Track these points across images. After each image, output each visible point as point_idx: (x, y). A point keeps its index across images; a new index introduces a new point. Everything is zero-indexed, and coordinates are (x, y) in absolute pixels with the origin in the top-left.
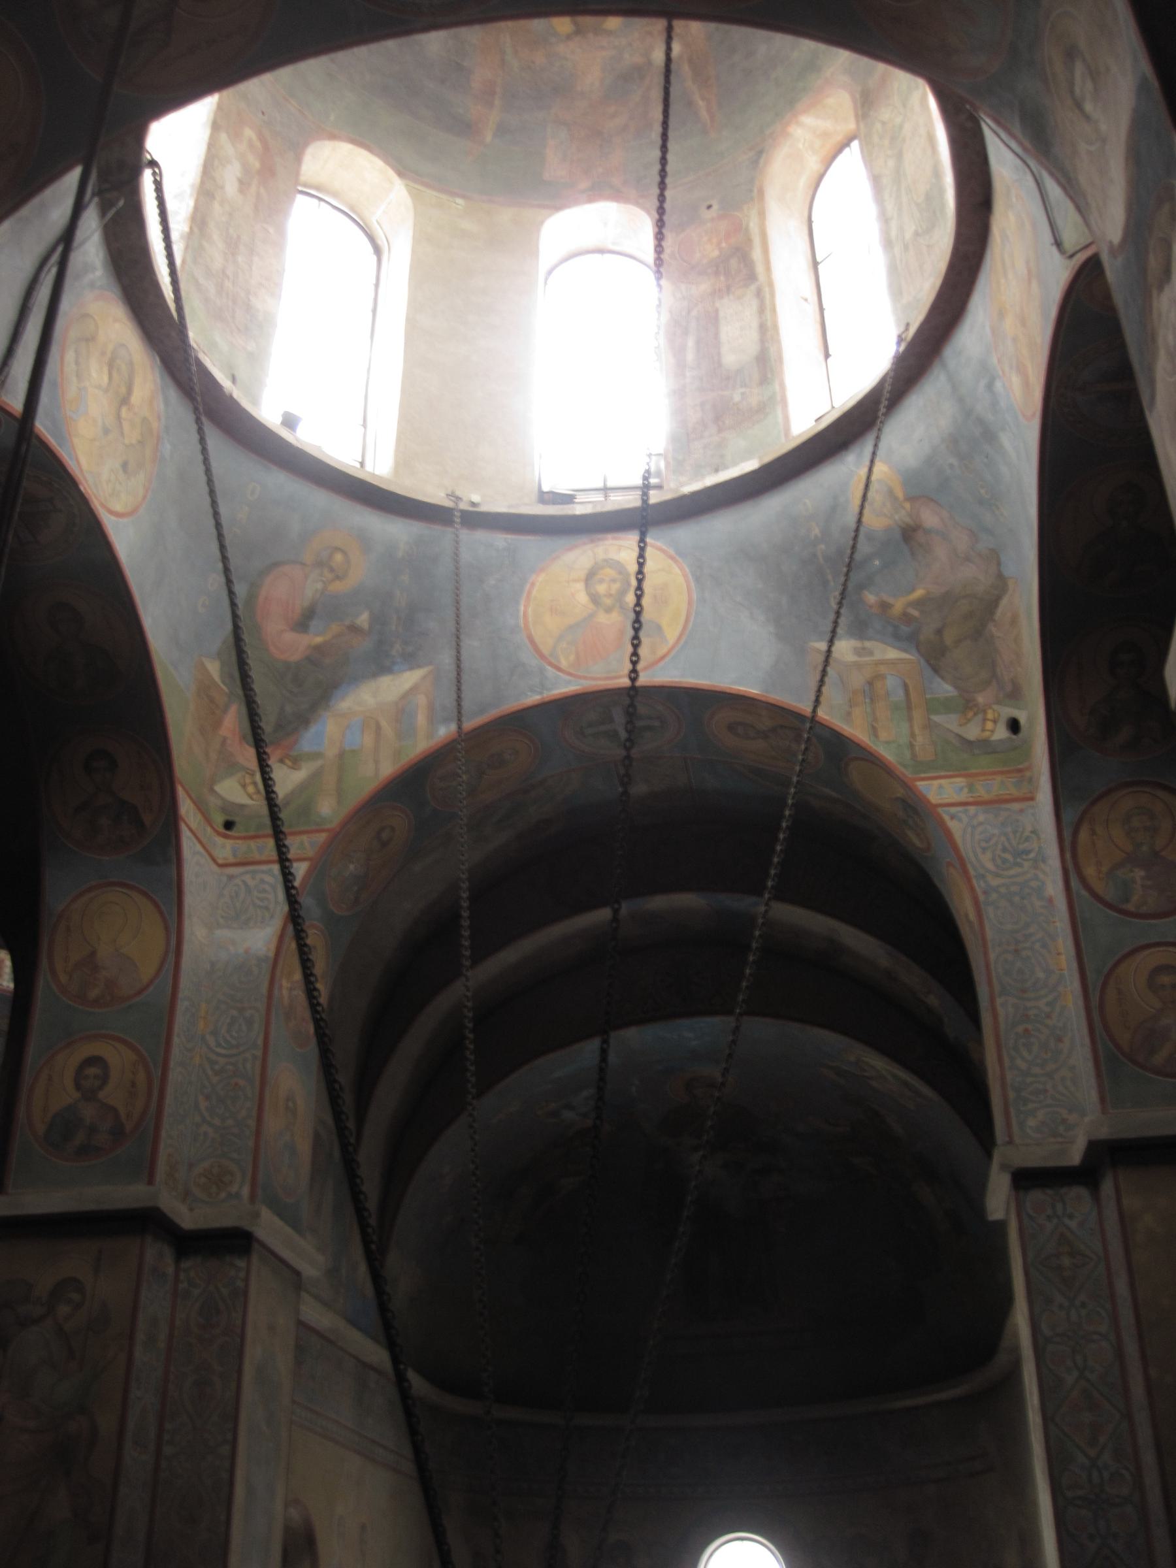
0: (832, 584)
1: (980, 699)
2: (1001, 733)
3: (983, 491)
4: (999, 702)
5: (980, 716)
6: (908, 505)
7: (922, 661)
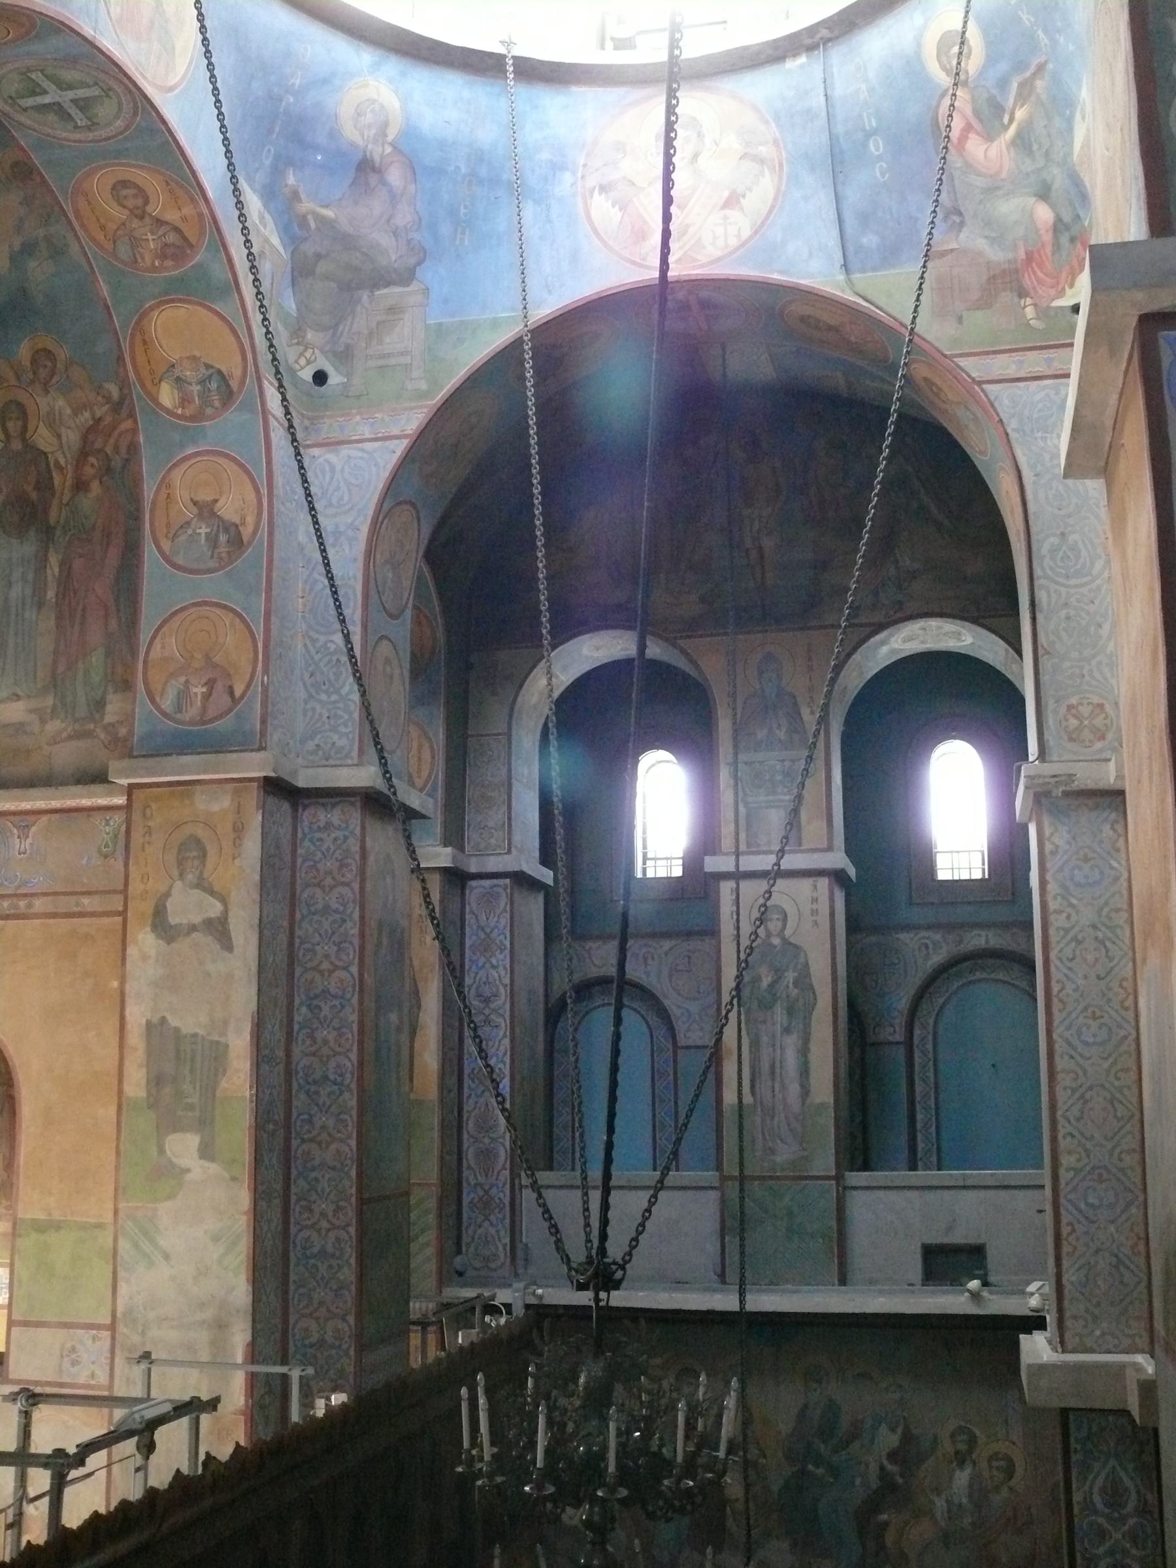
0: (274, 136)
1: (310, 335)
2: (307, 375)
3: (463, 210)
4: (322, 351)
5: (302, 348)
6: (389, 150)
7: (289, 269)
